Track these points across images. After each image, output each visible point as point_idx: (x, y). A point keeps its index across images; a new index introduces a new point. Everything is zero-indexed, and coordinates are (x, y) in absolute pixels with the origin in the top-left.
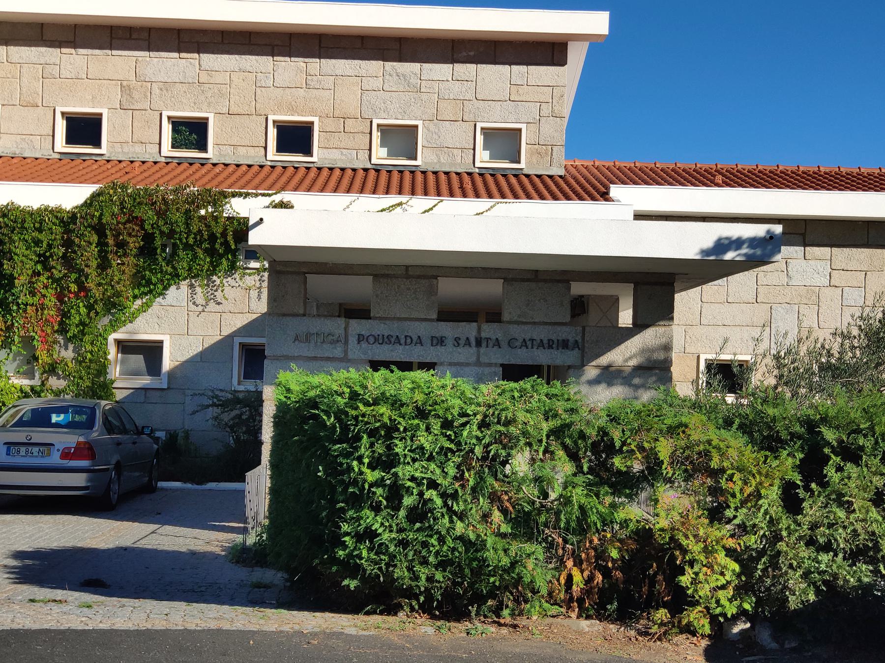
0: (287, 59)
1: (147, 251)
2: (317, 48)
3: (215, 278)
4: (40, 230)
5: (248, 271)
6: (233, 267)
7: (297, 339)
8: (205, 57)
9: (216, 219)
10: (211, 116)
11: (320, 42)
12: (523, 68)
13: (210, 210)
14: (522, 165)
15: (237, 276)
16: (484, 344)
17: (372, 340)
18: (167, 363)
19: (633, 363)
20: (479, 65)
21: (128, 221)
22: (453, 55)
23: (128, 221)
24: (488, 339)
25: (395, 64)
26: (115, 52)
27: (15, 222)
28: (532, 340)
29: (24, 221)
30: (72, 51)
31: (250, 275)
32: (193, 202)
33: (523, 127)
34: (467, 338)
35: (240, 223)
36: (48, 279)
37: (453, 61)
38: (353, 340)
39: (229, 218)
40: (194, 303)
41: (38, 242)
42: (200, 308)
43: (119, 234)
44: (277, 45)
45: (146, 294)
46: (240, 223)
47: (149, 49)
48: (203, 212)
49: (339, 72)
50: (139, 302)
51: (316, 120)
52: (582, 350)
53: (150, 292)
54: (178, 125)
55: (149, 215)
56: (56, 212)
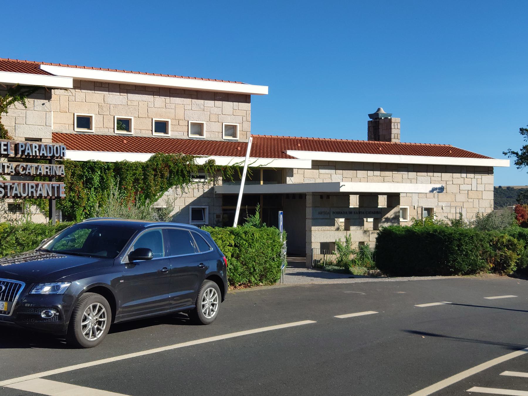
0: (159, 97)
2: (169, 93)
5: (193, 183)
7: (319, 213)
8: (129, 95)
10: (133, 118)
11: (170, 91)
12: (237, 103)
14: (238, 139)
15: (190, 184)
16: (360, 213)
17: (336, 213)
19: (392, 217)
20: (223, 102)
22: (214, 98)
24: (361, 212)
25: (195, 100)
26: (96, 92)
28: (371, 212)
30: (79, 91)
31: (194, 184)
33: (238, 125)
34: (357, 212)
37: (215, 100)
38: (332, 213)
40: (177, 194)
44: (155, 92)
47: (109, 91)
49: (177, 103)
51: (169, 120)
52: (381, 214)
54: (120, 121)
56: (140, 163)
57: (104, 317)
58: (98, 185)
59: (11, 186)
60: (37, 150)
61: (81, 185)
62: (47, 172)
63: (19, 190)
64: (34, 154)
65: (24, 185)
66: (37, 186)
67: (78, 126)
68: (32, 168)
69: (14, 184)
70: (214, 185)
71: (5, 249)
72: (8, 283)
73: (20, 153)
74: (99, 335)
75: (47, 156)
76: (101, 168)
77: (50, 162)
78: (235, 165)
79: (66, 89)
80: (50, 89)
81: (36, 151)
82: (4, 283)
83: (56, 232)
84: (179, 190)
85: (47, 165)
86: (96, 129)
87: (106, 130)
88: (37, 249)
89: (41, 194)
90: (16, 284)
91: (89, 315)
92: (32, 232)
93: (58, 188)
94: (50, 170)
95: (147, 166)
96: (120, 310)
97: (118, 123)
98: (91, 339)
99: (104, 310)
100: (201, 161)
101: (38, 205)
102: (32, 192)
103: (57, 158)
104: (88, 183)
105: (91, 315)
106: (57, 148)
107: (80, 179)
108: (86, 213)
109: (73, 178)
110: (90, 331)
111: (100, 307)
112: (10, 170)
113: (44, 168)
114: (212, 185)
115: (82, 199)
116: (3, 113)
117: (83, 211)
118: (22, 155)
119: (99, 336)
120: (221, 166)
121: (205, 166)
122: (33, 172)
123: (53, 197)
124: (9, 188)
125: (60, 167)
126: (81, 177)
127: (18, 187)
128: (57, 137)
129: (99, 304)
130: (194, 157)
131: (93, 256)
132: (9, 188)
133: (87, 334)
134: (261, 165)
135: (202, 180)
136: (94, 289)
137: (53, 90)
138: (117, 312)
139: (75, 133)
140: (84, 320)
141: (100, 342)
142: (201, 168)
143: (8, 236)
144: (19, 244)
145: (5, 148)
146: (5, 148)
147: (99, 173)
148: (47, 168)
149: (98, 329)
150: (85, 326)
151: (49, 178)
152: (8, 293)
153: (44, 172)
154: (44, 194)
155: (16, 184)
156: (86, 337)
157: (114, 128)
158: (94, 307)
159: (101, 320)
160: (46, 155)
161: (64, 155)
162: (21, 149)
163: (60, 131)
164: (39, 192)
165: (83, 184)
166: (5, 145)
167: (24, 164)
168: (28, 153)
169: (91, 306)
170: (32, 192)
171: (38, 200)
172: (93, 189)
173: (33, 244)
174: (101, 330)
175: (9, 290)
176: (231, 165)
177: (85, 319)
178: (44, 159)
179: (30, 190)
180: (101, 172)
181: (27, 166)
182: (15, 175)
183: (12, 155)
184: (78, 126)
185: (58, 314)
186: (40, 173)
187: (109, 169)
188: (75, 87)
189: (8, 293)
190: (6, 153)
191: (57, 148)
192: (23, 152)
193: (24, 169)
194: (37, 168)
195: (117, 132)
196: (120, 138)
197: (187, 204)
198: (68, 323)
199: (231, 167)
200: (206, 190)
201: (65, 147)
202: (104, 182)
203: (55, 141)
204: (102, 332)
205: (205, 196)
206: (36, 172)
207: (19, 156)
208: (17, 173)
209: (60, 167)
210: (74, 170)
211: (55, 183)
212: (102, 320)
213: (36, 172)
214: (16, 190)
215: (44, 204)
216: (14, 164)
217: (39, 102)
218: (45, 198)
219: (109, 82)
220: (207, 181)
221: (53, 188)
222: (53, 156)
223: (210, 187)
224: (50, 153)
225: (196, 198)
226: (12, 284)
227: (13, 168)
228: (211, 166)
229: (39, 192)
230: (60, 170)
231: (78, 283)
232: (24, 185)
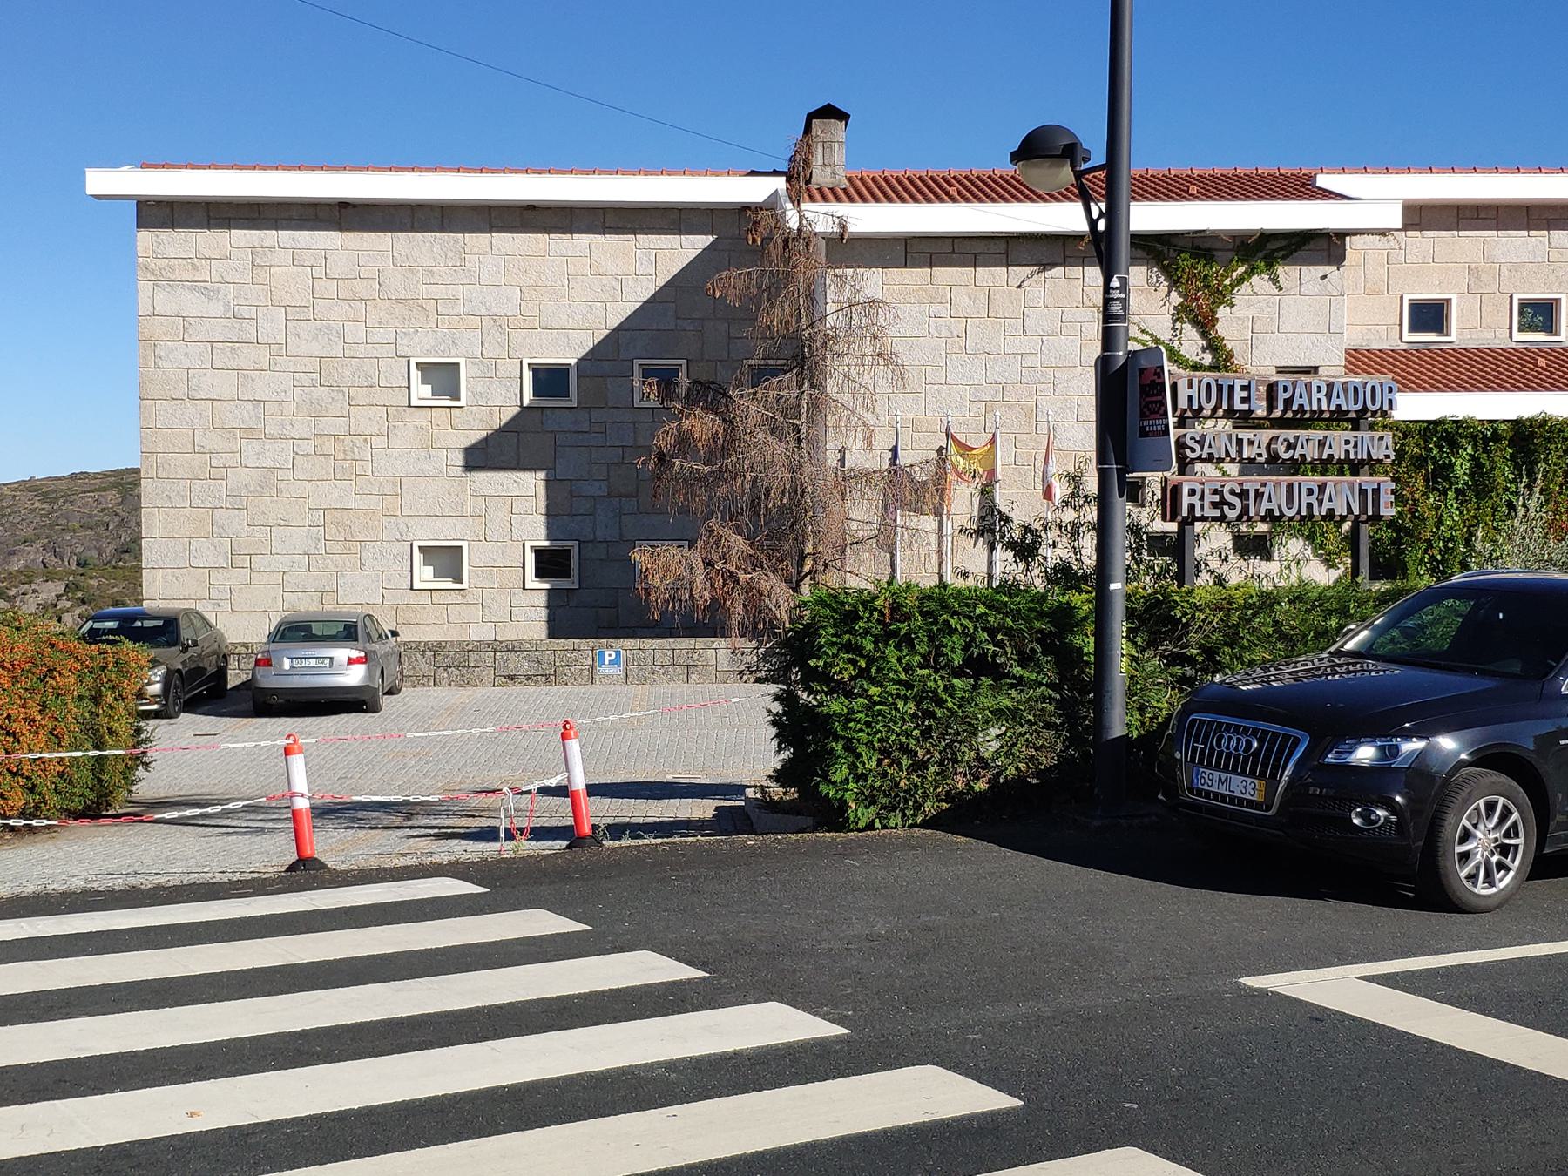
57: (1517, 836)
58: (1466, 483)
59: (1257, 490)
60: (1322, 395)
61: (1420, 484)
62: (1347, 452)
63: (1276, 500)
64: (1315, 408)
65: (1290, 486)
66: (1322, 488)
67: (1414, 328)
68: (1309, 443)
69: (1264, 485)
71: (1249, 649)
72: (1265, 733)
73: (1281, 407)
74: (1504, 881)
75: (1348, 412)
76: (1474, 438)
77: (1356, 428)
79: (1382, 233)
80: (1342, 235)
81: (1319, 400)
82: (1255, 731)
83: (1376, 608)
85: (1349, 435)
86: (1459, 334)
87: (1489, 334)
88: (1332, 649)
89: (1332, 510)
90: (1286, 738)
91: (1475, 826)
92: (1314, 607)
93: (1376, 492)
94: (1356, 446)
96: (1559, 818)
97: (1521, 313)
98: (1481, 889)
99: (1515, 816)
101: (1307, 538)
102: (1310, 506)
103: (1374, 414)
104: (1440, 476)
105: (1481, 826)
106: (1373, 388)
107: (1418, 468)
108: (1433, 558)
109: (1399, 465)
110: (1477, 868)
111: (1505, 807)
112: (1255, 450)
113: (1339, 442)
115: (1424, 520)
117: (1426, 551)
118: (1284, 412)
119: (1502, 885)
122: (1312, 453)
123: (1363, 517)
124: (1252, 494)
125: (1381, 438)
126: (1419, 462)
127: (1274, 492)
128: (1357, 359)
129: (1501, 800)
131: (1483, 673)
132: (1252, 494)
133: (1472, 877)
136: (1485, 759)
137: (1348, 239)
138: (1552, 824)
139: (1405, 347)
140: (1463, 840)
141: (1506, 899)
143: (1254, 615)
144: (1283, 637)
145: (1245, 394)
146: (1245, 394)
147: (1470, 450)
148: (1347, 442)
149: (1501, 866)
150: (1465, 857)
151: (1355, 467)
152: (1267, 757)
153: (1339, 454)
154: (1341, 510)
155: (1270, 485)
156: (1469, 885)
157: (1511, 328)
158: (1491, 807)
159: (1507, 841)
160: (1344, 408)
161: (1391, 408)
162: (1282, 397)
163: (1364, 344)
164: (1326, 505)
165: (1426, 479)
166: (1243, 388)
167: (1290, 434)
168: (1301, 406)
169: (1481, 802)
170: (1310, 506)
171: (1309, 526)
172: (1451, 494)
173: (1316, 637)
174: (1508, 869)
175: (1270, 750)
177: (1466, 836)
178: (1339, 417)
179: (1305, 499)
180: (1475, 447)
181: (1297, 438)
182: (1267, 462)
183: (1261, 412)
184: (1414, 328)
185: (1394, 818)
186: (1331, 456)
187: (1496, 437)
188: (1407, 227)
189: (1267, 757)
190: (1245, 407)
191: (1373, 388)
192: (1288, 403)
193: (1290, 446)
194: (1321, 444)
195: (1518, 336)
196: (1527, 355)
198: (1421, 843)
201: (1395, 386)
202: (1482, 475)
203: (1351, 370)
204: (1512, 874)
206: (1321, 453)
207: (1277, 414)
208: (1273, 458)
209: (1381, 438)
211: (1367, 481)
212: (1512, 842)
213: (1321, 453)
214: (1270, 500)
215: (1322, 534)
216: (1265, 435)
217: (1313, 272)
218: (1343, 519)
219: (1497, 202)
221: (1363, 492)
222: (1365, 410)
224: (1356, 403)
226: (1275, 735)
227: (1264, 446)
229: (1326, 505)
230: (1381, 446)
231: (1447, 743)
232: (1290, 486)
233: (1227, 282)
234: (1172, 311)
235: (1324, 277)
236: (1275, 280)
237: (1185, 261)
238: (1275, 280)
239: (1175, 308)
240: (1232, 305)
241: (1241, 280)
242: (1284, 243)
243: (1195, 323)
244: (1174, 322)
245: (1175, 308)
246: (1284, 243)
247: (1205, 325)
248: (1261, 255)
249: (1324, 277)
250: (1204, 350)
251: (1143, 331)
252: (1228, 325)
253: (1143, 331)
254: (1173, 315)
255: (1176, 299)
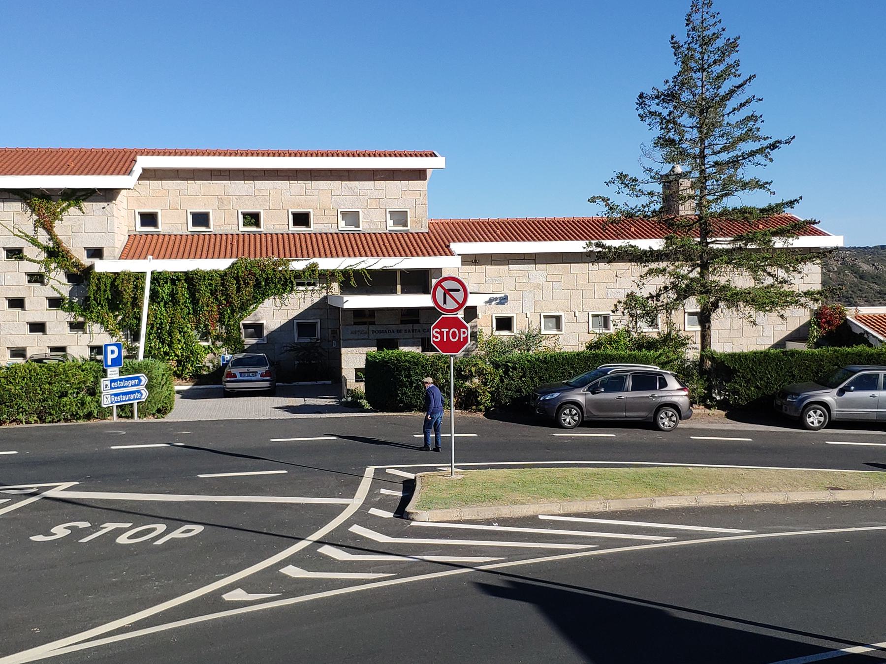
1: (258, 285)
3: (284, 295)
4: (211, 280)
6: (292, 289)
9: (286, 271)
13: (283, 267)
18: (265, 333)
21: (249, 274)
23: (249, 274)
27: (201, 277)
29: (205, 276)
32: (276, 265)
35: (296, 273)
36: (213, 299)
39: (291, 270)
41: (210, 285)
42: (279, 308)
43: (245, 280)
45: (255, 303)
46: (296, 273)
48: (280, 269)
50: (252, 307)
53: (257, 302)
55: (258, 272)
70: (327, 293)
78: (348, 268)
84: (278, 300)
95: (226, 274)
100: (299, 265)
114: (324, 293)
116: (57, 221)
120: (327, 270)
121: (303, 271)
130: (289, 261)
134: (385, 267)
135: (311, 288)
142: (298, 275)
176: (342, 268)
197: (290, 318)
199: (341, 271)
200: (316, 300)
205: (315, 307)
210: (137, 283)
220: (316, 288)
223: (322, 296)
225: (303, 310)
228: (313, 271)
233: (59, 210)
234: (34, 223)
235: (103, 208)
236: (81, 209)
237: (36, 201)
238: (81, 209)
239: (35, 221)
240: (62, 220)
241: (63, 210)
242: (83, 193)
243: (44, 228)
244: (35, 227)
245: (35, 221)
246: (83, 193)
247: (49, 230)
248: (74, 198)
249: (103, 208)
250: (50, 240)
251: (20, 232)
252: (59, 228)
253: (20, 232)
254: (35, 224)
255: (35, 217)
